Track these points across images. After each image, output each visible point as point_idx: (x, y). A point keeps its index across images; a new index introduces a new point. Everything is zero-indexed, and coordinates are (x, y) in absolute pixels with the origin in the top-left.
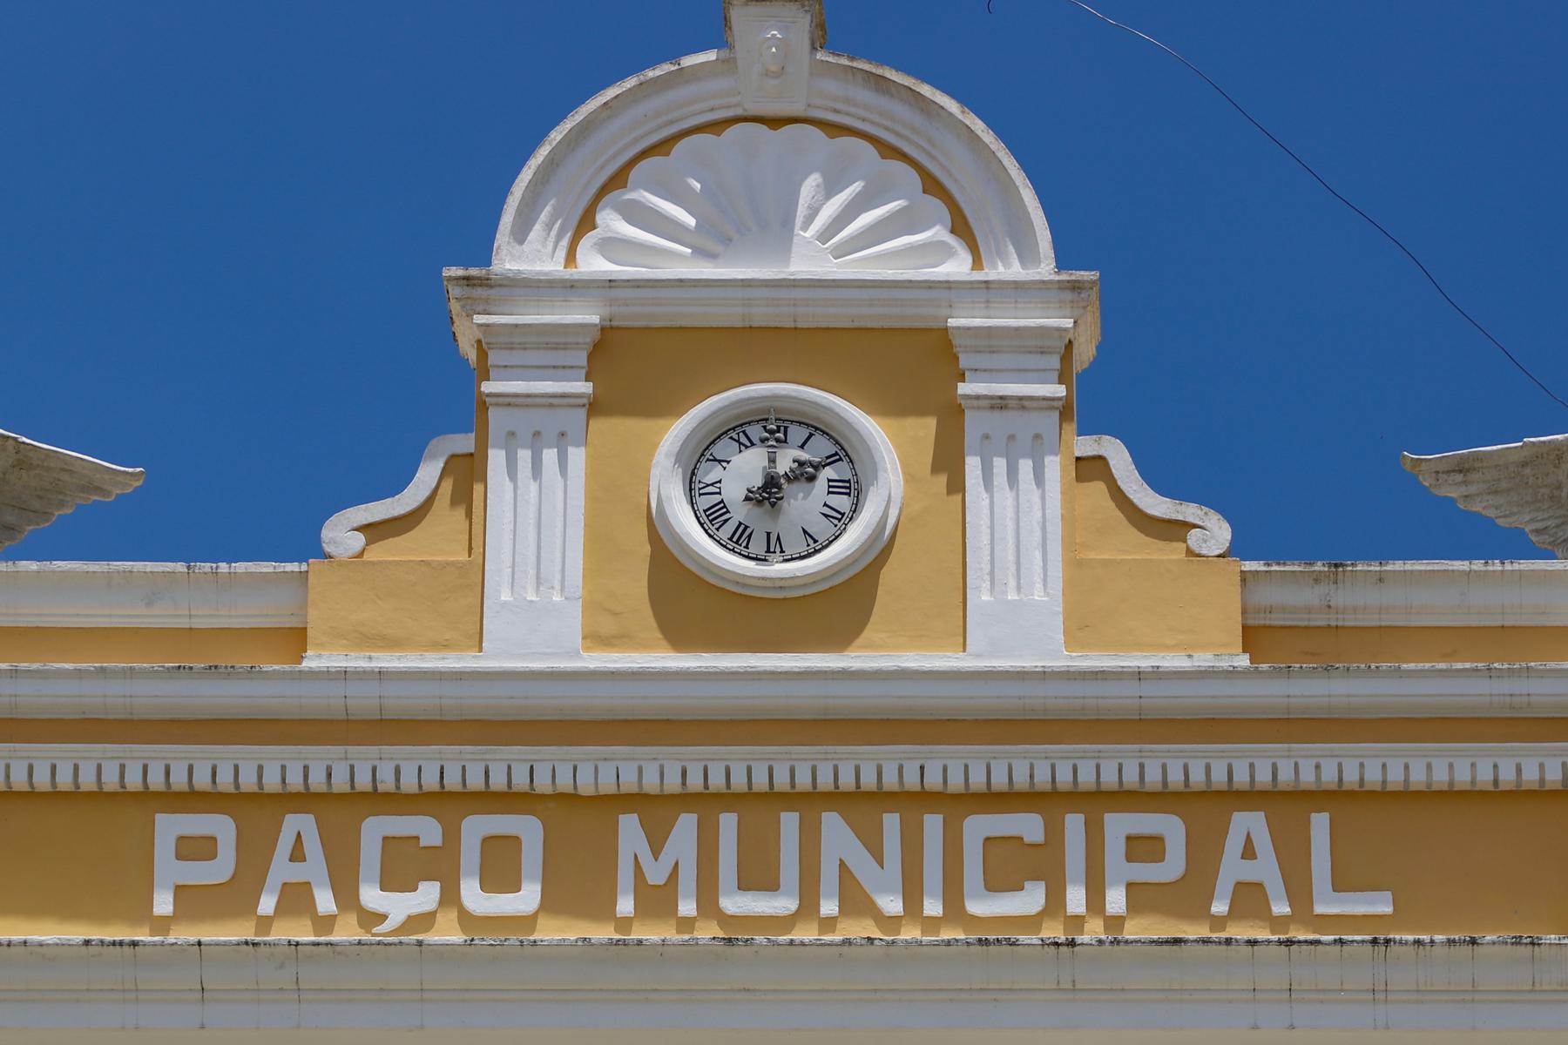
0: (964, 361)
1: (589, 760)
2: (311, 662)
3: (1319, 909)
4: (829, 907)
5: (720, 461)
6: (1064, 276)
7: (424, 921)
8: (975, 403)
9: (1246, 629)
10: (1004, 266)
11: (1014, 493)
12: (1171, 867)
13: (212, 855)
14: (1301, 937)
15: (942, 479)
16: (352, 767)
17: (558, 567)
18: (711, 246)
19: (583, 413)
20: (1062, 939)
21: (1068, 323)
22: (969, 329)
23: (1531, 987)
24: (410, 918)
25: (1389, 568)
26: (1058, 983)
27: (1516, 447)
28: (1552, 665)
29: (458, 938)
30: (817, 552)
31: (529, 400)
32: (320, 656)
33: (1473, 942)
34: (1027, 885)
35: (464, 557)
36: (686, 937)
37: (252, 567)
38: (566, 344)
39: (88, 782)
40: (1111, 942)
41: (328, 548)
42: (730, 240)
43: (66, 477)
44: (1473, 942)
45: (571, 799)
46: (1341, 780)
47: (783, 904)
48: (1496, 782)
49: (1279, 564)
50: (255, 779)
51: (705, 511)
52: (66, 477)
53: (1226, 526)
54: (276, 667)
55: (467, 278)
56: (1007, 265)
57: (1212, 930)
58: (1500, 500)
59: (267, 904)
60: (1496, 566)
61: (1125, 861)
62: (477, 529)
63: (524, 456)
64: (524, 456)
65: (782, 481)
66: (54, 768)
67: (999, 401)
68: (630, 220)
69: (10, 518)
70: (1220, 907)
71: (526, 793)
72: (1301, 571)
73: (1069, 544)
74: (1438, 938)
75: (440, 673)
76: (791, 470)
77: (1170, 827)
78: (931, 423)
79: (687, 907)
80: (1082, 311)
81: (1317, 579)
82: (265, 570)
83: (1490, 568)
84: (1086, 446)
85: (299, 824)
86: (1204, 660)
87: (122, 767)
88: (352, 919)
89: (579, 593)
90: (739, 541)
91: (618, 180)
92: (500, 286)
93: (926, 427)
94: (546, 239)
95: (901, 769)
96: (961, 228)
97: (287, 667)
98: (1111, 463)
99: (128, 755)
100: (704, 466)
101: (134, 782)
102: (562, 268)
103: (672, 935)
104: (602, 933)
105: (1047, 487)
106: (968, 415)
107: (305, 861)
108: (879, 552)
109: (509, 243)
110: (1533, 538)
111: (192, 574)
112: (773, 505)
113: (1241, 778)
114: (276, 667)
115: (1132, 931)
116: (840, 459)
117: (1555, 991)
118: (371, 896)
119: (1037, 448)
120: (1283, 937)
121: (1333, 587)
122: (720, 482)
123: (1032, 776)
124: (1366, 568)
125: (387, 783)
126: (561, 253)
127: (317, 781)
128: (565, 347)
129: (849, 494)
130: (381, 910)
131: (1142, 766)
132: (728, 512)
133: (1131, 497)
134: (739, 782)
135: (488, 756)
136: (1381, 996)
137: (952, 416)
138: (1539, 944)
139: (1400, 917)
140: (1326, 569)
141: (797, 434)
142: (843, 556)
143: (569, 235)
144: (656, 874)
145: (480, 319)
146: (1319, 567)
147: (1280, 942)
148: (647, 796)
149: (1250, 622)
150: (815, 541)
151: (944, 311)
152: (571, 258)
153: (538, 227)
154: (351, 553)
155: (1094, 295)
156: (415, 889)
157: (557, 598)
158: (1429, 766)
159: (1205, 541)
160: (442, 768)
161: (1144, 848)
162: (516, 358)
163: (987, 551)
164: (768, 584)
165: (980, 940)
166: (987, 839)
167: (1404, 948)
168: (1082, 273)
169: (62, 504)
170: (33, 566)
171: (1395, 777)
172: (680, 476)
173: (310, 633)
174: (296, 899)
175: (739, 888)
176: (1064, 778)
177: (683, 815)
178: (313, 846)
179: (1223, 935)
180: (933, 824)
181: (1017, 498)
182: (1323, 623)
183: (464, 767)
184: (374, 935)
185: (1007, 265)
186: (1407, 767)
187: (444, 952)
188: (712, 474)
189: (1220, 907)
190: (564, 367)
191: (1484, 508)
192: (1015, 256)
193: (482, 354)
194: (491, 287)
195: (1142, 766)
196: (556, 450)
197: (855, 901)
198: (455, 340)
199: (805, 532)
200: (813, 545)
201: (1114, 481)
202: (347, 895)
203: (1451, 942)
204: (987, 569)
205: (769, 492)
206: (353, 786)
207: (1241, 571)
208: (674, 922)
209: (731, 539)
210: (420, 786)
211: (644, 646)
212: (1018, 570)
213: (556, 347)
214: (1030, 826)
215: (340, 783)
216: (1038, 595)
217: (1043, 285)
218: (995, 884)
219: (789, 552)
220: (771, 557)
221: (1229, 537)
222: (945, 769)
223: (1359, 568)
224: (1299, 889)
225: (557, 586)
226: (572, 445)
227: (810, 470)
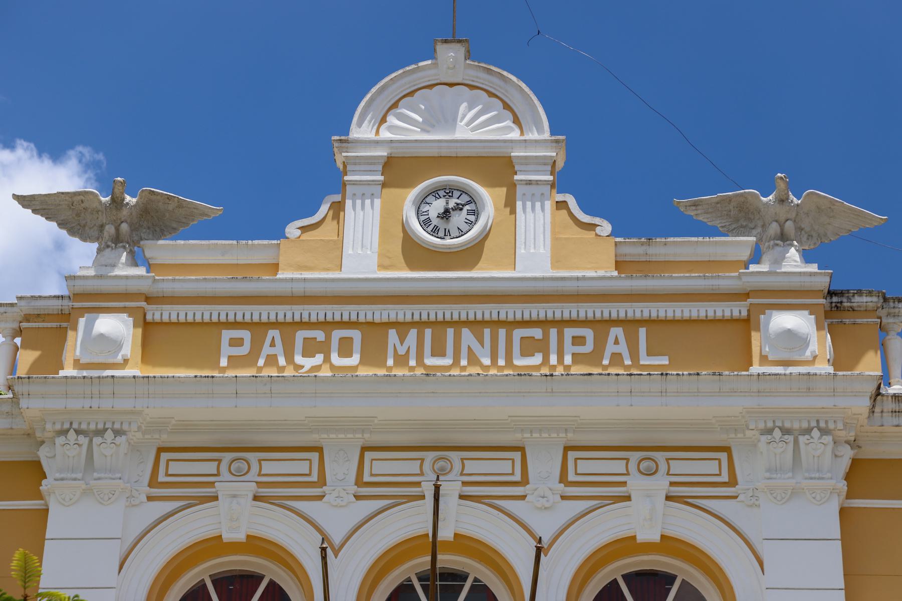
0: (517, 168)
1: (378, 310)
2: (280, 276)
3: (642, 363)
4: (464, 362)
5: (428, 204)
6: (553, 138)
7: (317, 368)
8: (520, 182)
9: (616, 262)
10: (531, 134)
11: (534, 214)
12: (588, 348)
13: (242, 345)
14: (635, 373)
15: (508, 210)
16: (293, 313)
17: (370, 241)
18: (428, 128)
19: (380, 187)
20: (548, 374)
21: (554, 154)
22: (518, 156)
23: (718, 391)
24: (312, 367)
25: (668, 240)
26: (546, 389)
27: (714, 197)
28: (727, 274)
29: (329, 374)
30: (462, 235)
31: (361, 183)
32: (283, 273)
33: (698, 374)
34: (536, 354)
35: (336, 238)
36: (412, 373)
37: (260, 242)
38: (374, 162)
39: (198, 319)
40: (566, 375)
41: (288, 235)
42: (434, 126)
43: (195, 211)
44: (698, 374)
45: (372, 324)
46: (650, 316)
47: (447, 361)
48: (707, 316)
49: (629, 239)
50: (258, 317)
51: (423, 221)
52: (195, 211)
53: (610, 225)
54: (267, 277)
55: (340, 140)
56: (533, 134)
57: (603, 370)
58: (709, 216)
59: (261, 362)
60: (707, 239)
61: (571, 344)
62: (341, 228)
63: (359, 202)
64: (359, 202)
65: (451, 210)
66: (186, 314)
67: (529, 182)
68: (399, 119)
69: (174, 225)
70: (606, 362)
71: (355, 322)
72: (637, 242)
73: (553, 232)
74: (685, 373)
75: (326, 279)
76: (454, 207)
77: (588, 333)
78: (504, 190)
79: (413, 363)
80: (559, 150)
81: (642, 244)
82: (265, 243)
83: (705, 240)
84: (560, 197)
85: (274, 333)
86: (601, 273)
87: (211, 313)
88: (291, 367)
89: (377, 250)
90: (435, 231)
91: (395, 105)
92: (352, 142)
93: (503, 191)
94: (369, 126)
95: (491, 312)
96: (517, 121)
97: (271, 277)
98: (569, 203)
99: (213, 309)
100: (423, 205)
101: (215, 319)
102: (374, 136)
103: (407, 373)
104: (382, 372)
105: (546, 212)
106: (518, 186)
107: (275, 346)
108: (485, 236)
109: (356, 128)
110: (721, 229)
111: (239, 245)
112: (447, 219)
113: (614, 315)
114: (267, 277)
115: (574, 370)
116: (472, 203)
117: (728, 392)
118: (299, 359)
119: (542, 198)
120: (629, 373)
121: (648, 247)
122: (428, 211)
123: (538, 315)
124: (660, 240)
125: (306, 319)
126: (374, 131)
127: (281, 318)
128: (374, 164)
129: (474, 215)
130: (302, 364)
131: (578, 311)
132: (431, 221)
133: (576, 215)
134: (432, 318)
135: (342, 309)
136: (665, 394)
137: (512, 187)
138: (722, 375)
139: (671, 365)
140: (646, 240)
141: (457, 194)
142: (471, 237)
143: (377, 125)
144: (402, 351)
145: (344, 154)
146: (643, 240)
147: (627, 375)
148: (399, 322)
149: (618, 259)
150: (462, 232)
151: (510, 150)
152: (377, 132)
153: (366, 122)
154: (296, 237)
155: (564, 144)
156: (314, 357)
157: (369, 252)
158: (682, 311)
159: (602, 231)
160: (326, 313)
161: (578, 341)
162: (357, 168)
163: (523, 235)
164: (444, 247)
165: (518, 374)
166: (522, 338)
167: (672, 377)
168: (560, 137)
169: (193, 220)
170: (182, 242)
171: (670, 315)
172: (414, 209)
173: (280, 265)
174: (271, 360)
175: (431, 356)
176: (550, 316)
177: (412, 330)
178: (278, 341)
179: (607, 372)
180: (502, 332)
181: (535, 216)
182: (645, 260)
183: (333, 313)
184: (299, 373)
185: (533, 134)
186: (674, 311)
187: (324, 379)
188: (425, 208)
189: (606, 362)
190: (374, 171)
191: (703, 219)
192: (536, 131)
193: (345, 166)
194: (349, 143)
195: (578, 311)
196: (370, 200)
197: (473, 360)
198: (335, 162)
199: (458, 228)
200: (461, 233)
201: (570, 210)
202: (290, 359)
203: (690, 374)
204: (524, 241)
205: (446, 214)
206: (293, 320)
207: (615, 242)
208: (408, 368)
209: (432, 231)
210: (318, 320)
211: (400, 269)
212: (535, 241)
213: (371, 164)
214: (537, 333)
215: (289, 319)
216: (542, 251)
217: (545, 141)
218: (525, 354)
219: (452, 235)
220: (446, 237)
221: (611, 230)
222: (507, 313)
223: (658, 240)
224: (634, 355)
225: (369, 248)
226: (376, 198)
227: (461, 206)
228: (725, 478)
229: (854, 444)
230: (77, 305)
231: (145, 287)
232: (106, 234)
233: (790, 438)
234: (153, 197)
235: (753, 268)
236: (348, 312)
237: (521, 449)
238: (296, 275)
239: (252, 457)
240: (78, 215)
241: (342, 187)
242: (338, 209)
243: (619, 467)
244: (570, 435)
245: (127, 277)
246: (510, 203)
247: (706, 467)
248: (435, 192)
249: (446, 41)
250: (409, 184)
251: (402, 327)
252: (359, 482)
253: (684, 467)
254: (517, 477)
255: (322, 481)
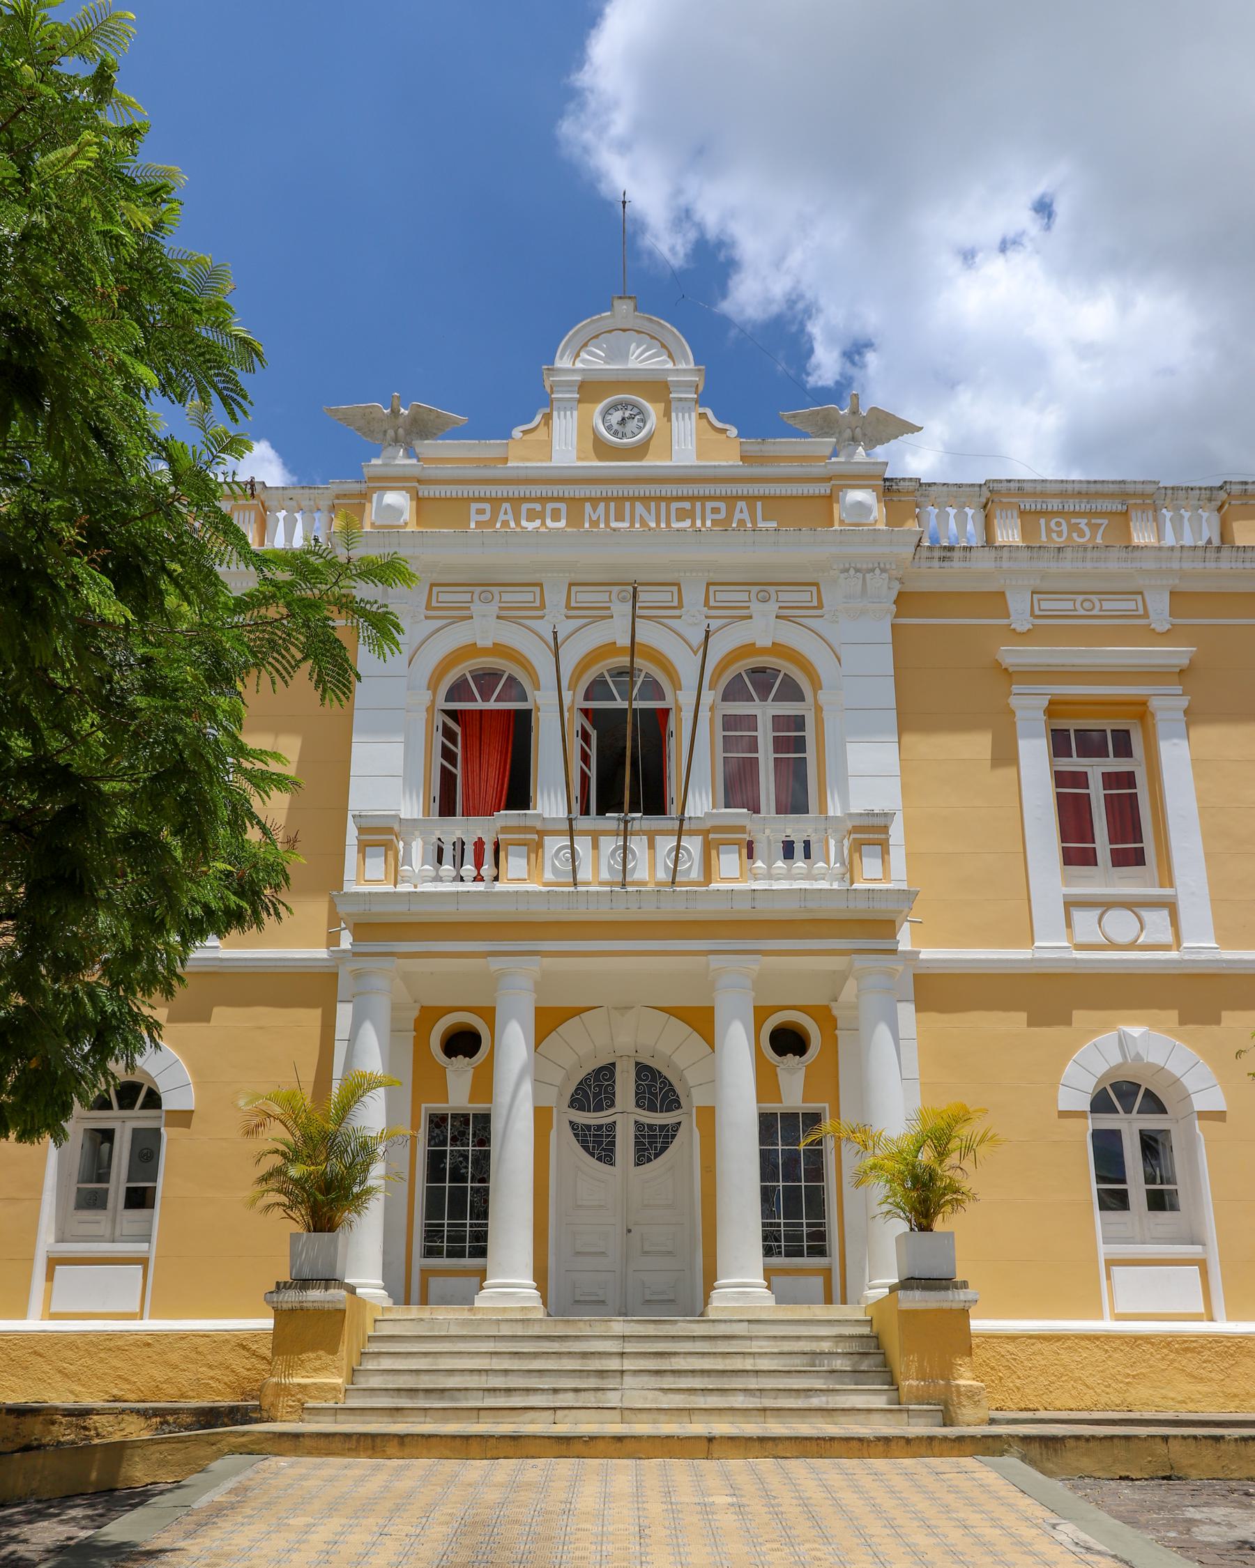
2: (509, 464)
12: (723, 515)
47: (626, 525)
59: (498, 525)
63: (562, 413)
64: (562, 413)
77: (722, 505)
79: (602, 526)
81: (759, 443)
84: (701, 410)
86: (731, 463)
90: (615, 434)
91: (586, 345)
96: (670, 356)
101: (465, 495)
108: (650, 437)
113: (740, 493)
118: (524, 523)
119: (690, 410)
125: (528, 495)
127: (511, 495)
137: (668, 403)
144: (594, 518)
161: (715, 510)
170: (441, 442)
174: (505, 524)
178: (509, 511)
180: (663, 505)
188: (609, 417)
193: (552, 388)
197: (643, 523)
202: (518, 523)
214: (687, 505)
215: (516, 495)
217: (691, 370)
218: (679, 519)
228: (815, 603)
229: (901, 581)
230: (372, 485)
231: (416, 472)
232: (388, 437)
233: (860, 575)
234: (420, 410)
235: (834, 459)
236: (557, 490)
237: (678, 585)
238: (521, 464)
239: (495, 590)
240: (368, 423)
241: (549, 402)
242: (548, 418)
243: (744, 596)
244: (711, 574)
245: (404, 465)
246: (667, 414)
247: (804, 596)
248: (614, 407)
249: (620, 298)
250: (597, 400)
251: (594, 501)
252: (568, 607)
253: (789, 596)
254: (675, 604)
255: (543, 606)
